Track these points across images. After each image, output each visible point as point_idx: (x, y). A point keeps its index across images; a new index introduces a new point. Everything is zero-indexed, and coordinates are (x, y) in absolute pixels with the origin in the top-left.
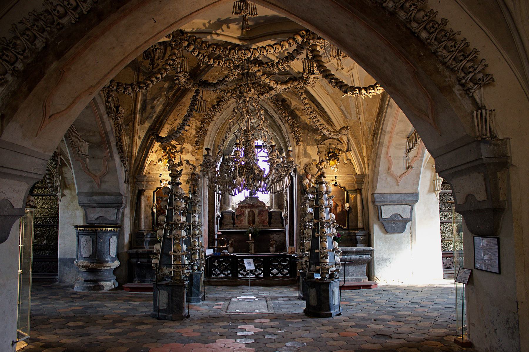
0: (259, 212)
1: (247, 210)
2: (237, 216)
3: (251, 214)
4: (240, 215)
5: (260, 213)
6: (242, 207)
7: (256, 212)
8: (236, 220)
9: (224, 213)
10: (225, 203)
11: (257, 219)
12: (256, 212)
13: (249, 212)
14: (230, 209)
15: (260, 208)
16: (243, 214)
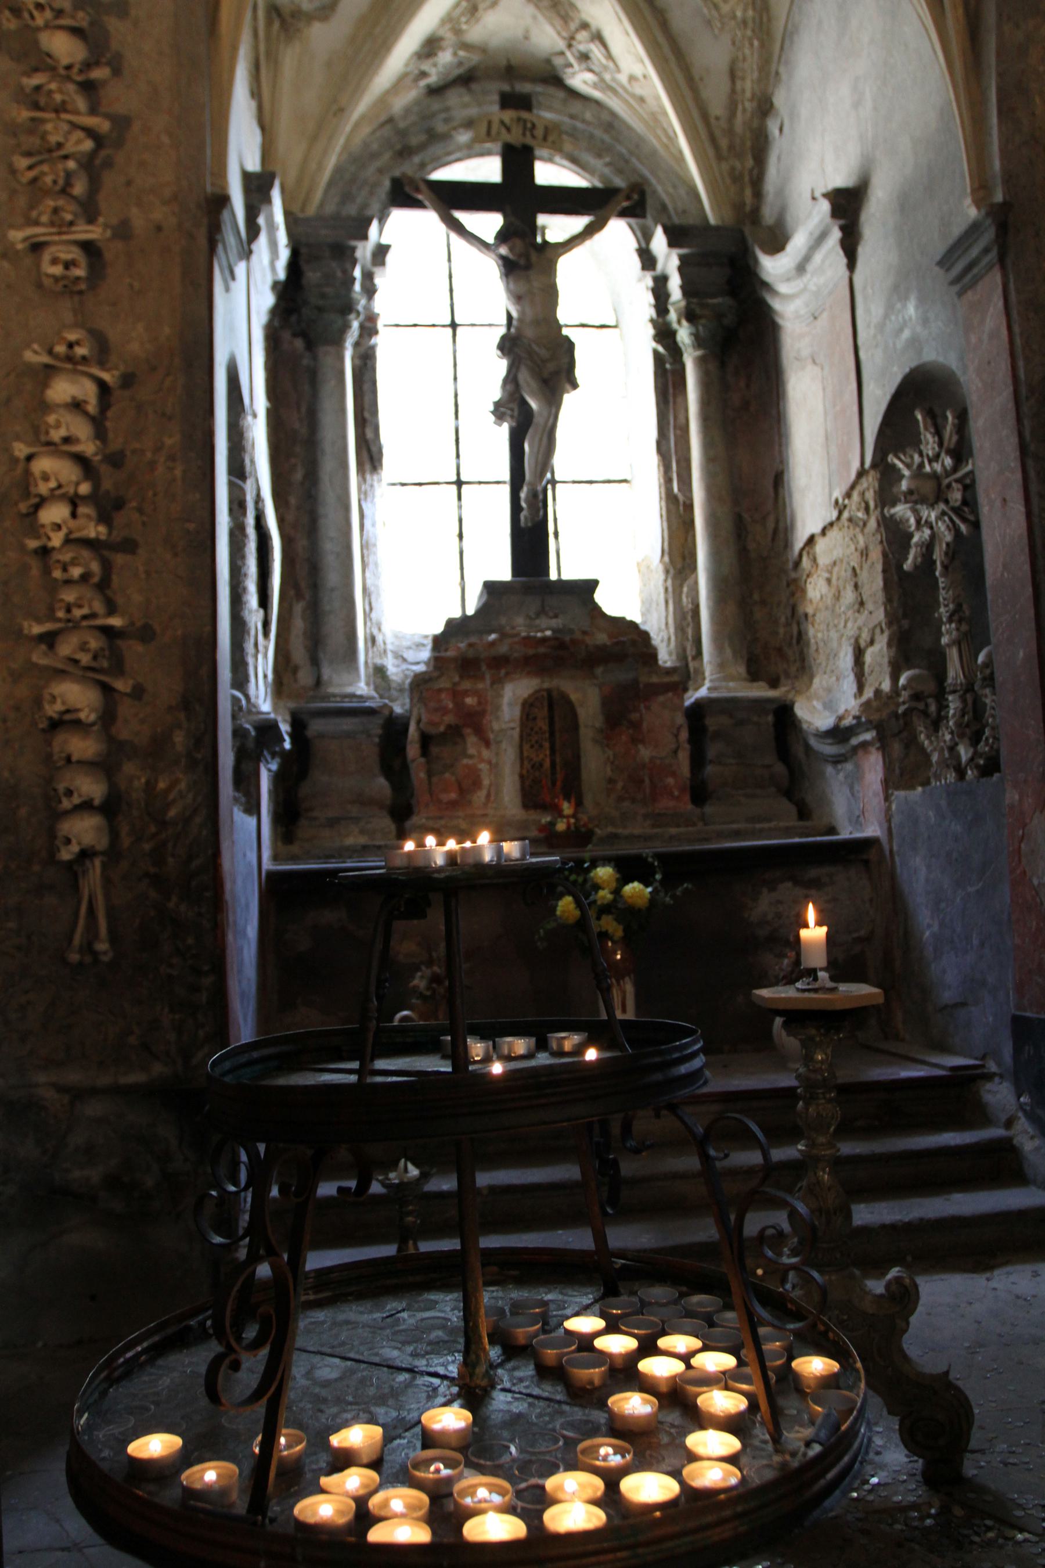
0: (607, 703)
1: (512, 695)
2: (426, 740)
3: (550, 719)
4: (454, 734)
5: (621, 712)
6: (468, 666)
7: (587, 698)
8: (418, 774)
9: (316, 727)
10: (315, 642)
11: (594, 762)
12: (587, 698)
13: (528, 706)
14: (362, 687)
15: (620, 675)
16: (473, 722)
